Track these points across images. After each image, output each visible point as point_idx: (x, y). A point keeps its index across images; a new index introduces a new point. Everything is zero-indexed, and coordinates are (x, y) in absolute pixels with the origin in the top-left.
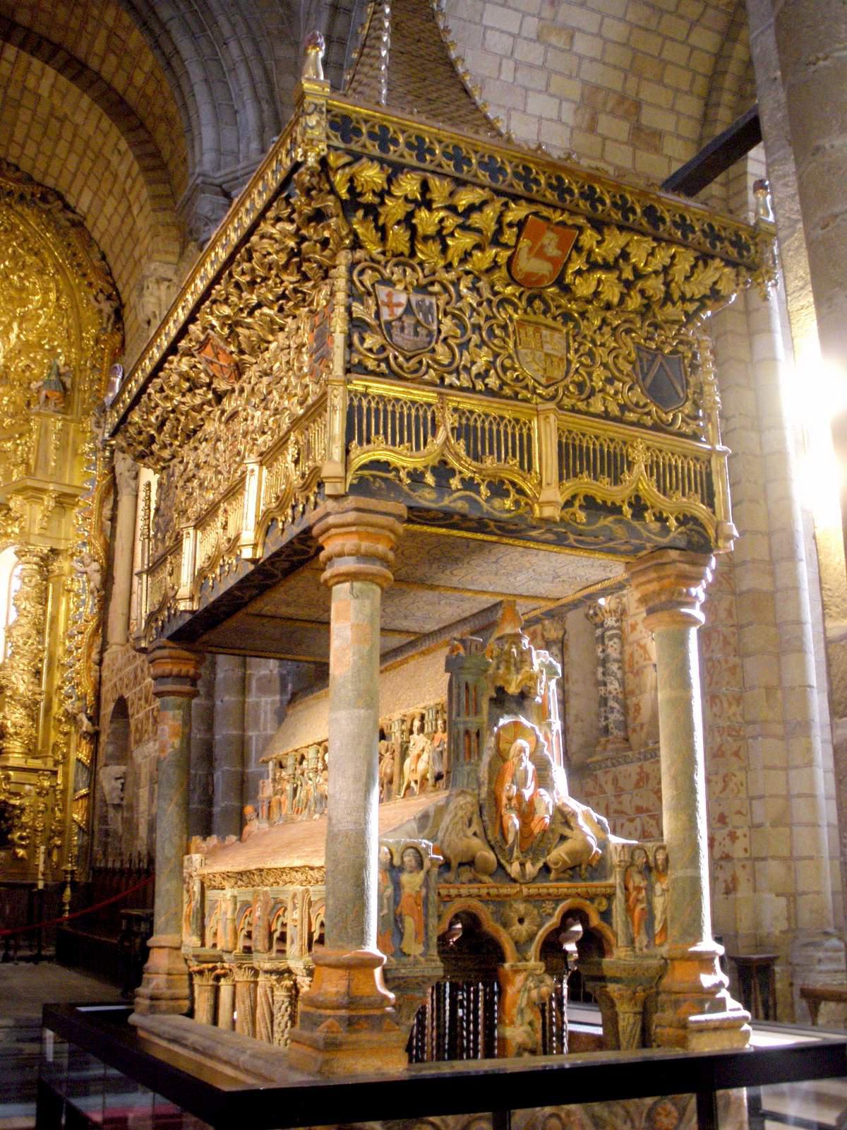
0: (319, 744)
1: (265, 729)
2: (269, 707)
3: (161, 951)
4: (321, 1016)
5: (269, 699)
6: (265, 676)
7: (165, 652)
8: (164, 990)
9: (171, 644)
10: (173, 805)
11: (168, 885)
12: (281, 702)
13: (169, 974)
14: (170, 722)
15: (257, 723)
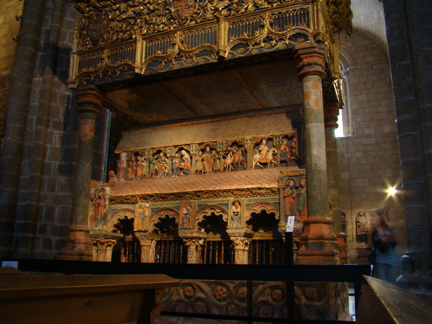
0: (175, 146)
1: (55, 145)
2: (57, 135)
3: (80, 233)
4: (326, 243)
5: (58, 132)
6: (57, 121)
7: (94, 92)
8: (84, 251)
9: (97, 89)
10: (89, 164)
11: (85, 201)
12: (64, 134)
13: (86, 244)
14: (90, 125)
15: (51, 142)
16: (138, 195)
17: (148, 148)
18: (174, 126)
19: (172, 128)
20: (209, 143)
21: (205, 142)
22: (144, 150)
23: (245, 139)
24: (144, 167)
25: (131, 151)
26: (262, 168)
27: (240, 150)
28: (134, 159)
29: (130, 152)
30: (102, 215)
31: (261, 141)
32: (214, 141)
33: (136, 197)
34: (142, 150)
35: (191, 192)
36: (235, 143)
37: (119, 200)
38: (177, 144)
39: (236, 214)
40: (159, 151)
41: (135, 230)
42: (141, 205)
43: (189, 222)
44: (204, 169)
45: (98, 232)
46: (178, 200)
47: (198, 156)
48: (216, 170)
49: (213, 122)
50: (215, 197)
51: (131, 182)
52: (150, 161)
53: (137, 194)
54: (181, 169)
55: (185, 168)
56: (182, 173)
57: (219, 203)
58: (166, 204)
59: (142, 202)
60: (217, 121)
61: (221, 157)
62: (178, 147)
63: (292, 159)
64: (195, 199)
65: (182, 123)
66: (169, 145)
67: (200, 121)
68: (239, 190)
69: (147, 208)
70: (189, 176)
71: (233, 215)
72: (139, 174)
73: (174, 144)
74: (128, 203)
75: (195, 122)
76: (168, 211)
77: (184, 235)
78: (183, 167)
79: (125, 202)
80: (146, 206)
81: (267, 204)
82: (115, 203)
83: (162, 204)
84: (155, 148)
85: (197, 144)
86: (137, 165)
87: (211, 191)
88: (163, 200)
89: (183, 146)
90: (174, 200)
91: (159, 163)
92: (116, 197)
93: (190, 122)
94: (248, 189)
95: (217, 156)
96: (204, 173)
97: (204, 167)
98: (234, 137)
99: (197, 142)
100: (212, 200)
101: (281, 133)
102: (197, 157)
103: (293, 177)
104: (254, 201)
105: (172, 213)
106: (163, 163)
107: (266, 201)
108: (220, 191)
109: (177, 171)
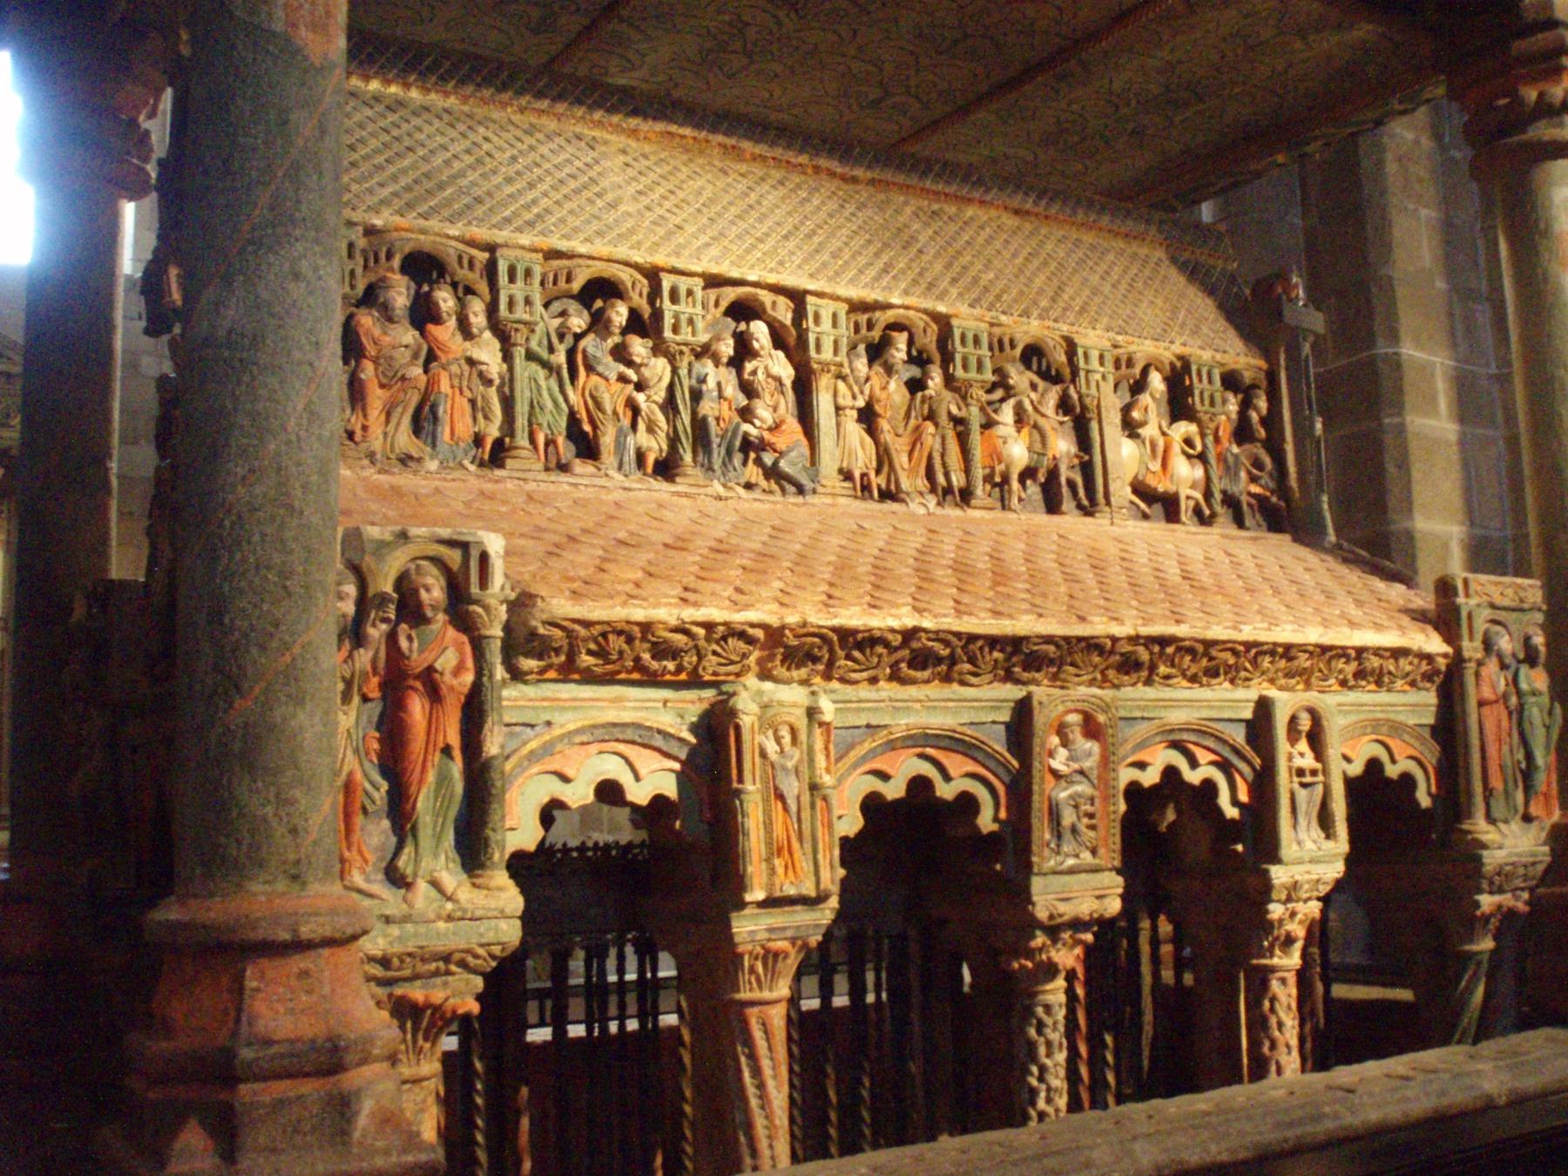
16: (774, 635)
17: (525, 240)
18: (618, 129)
19: (606, 143)
20: (911, 313)
21: (895, 300)
22: (491, 248)
23: (1077, 339)
24: (488, 382)
25: (370, 231)
26: (1145, 517)
27: (1053, 395)
28: (400, 295)
29: (361, 243)
30: (443, 778)
31: (1145, 371)
32: (942, 308)
33: (751, 641)
34: (472, 243)
35: (1114, 640)
36: (1032, 355)
37: (601, 653)
38: (735, 274)
39: (1308, 779)
40: (601, 290)
41: (757, 894)
42: (781, 704)
43: (1092, 827)
44: (878, 472)
45: (445, 936)
46: (1009, 677)
47: (851, 380)
48: (948, 491)
49: (855, 180)
50: (1204, 680)
51: (404, 479)
52: (534, 345)
53: (774, 621)
54: (747, 445)
55: (780, 442)
56: (753, 473)
57: (1214, 714)
58: (929, 705)
59: (765, 675)
60: (872, 182)
61: (975, 416)
62: (730, 294)
63: (1249, 494)
64: (1105, 682)
65: (674, 128)
66: (680, 264)
67: (778, 152)
68: (1324, 649)
69: (821, 724)
70: (810, 499)
71: (1296, 786)
72: (457, 422)
73: (706, 265)
74: (652, 680)
75: (747, 145)
76: (929, 751)
77: (1062, 908)
78: (766, 435)
79: (638, 665)
80: (812, 713)
81: (1396, 728)
82: (542, 671)
83: (897, 707)
84: (570, 256)
85: (848, 301)
86: (431, 357)
87: (1209, 644)
88: (919, 675)
89: (766, 297)
90: (990, 677)
91: (590, 369)
92: (587, 624)
93: (720, 138)
94: (1360, 651)
95: (954, 410)
96: (888, 495)
97: (884, 458)
98: (1026, 313)
99: (855, 293)
100: (1186, 694)
101: (1218, 357)
102: (841, 385)
103: (1504, 613)
104: (1350, 712)
105: (957, 764)
106: (623, 379)
107: (1392, 716)
108: (1249, 645)
109: (729, 453)
